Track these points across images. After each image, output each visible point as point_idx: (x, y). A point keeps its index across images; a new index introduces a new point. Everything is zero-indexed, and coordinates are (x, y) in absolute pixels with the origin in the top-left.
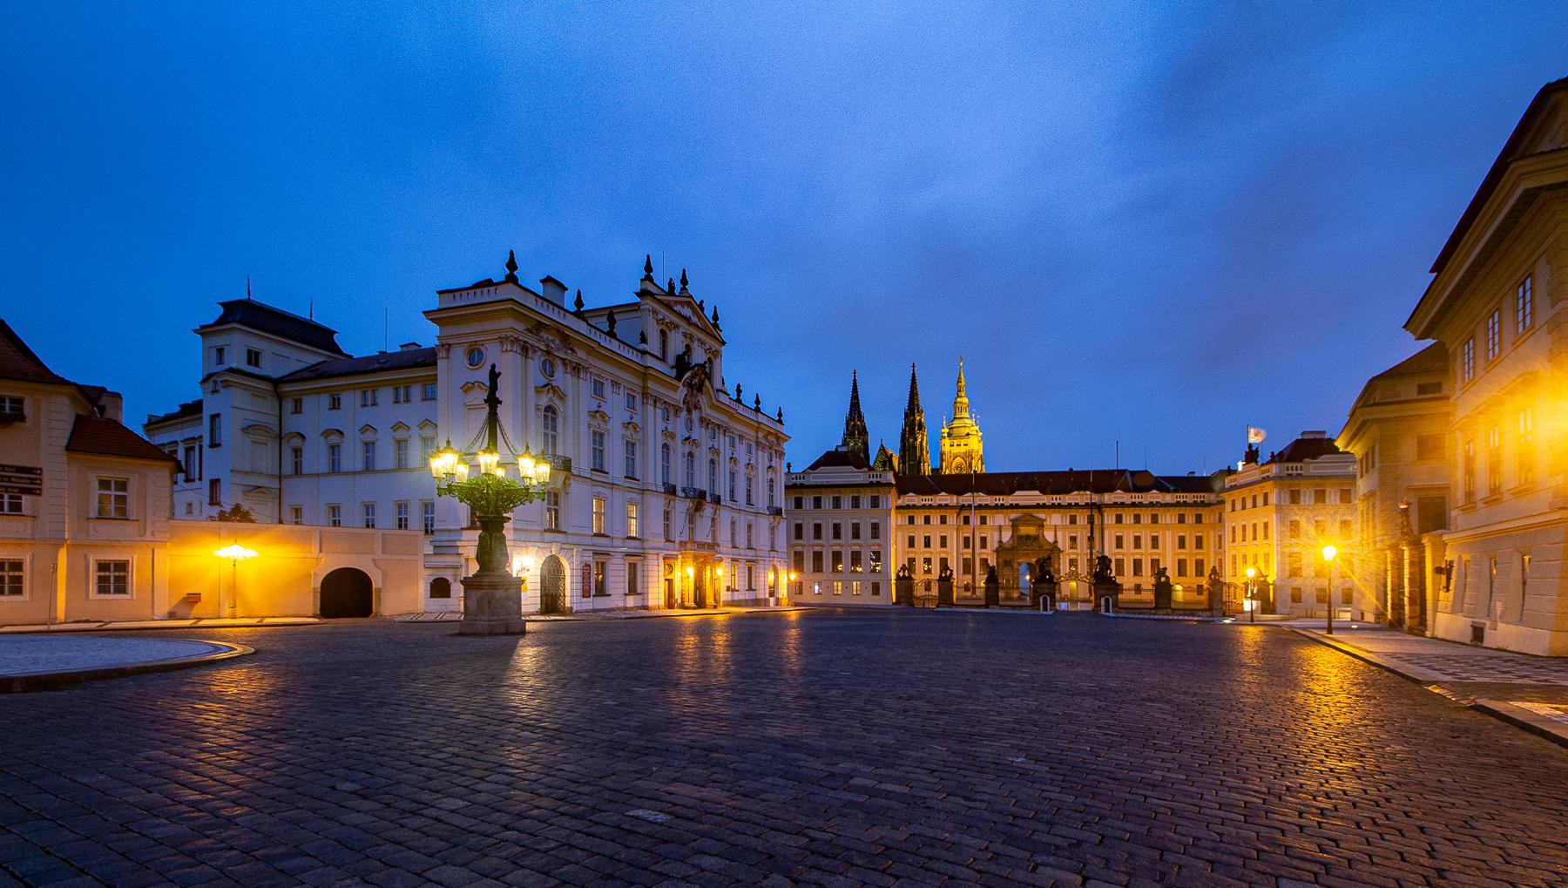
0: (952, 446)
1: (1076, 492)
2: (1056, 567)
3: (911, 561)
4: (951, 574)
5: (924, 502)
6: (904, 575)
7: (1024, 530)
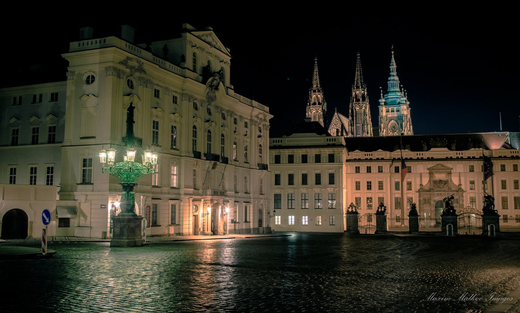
0: (388, 111)
1: (473, 149)
2: (461, 203)
3: (358, 200)
4: (385, 210)
5: (366, 157)
6: (352, 211)
7: (438, 176)
